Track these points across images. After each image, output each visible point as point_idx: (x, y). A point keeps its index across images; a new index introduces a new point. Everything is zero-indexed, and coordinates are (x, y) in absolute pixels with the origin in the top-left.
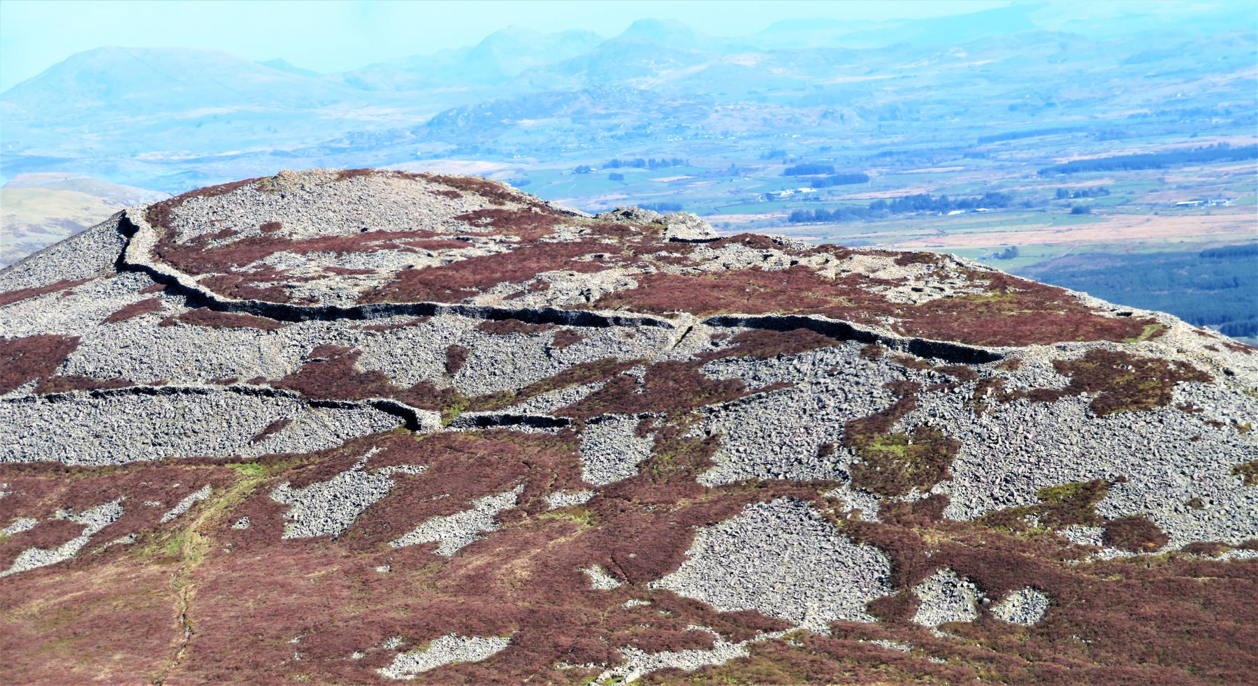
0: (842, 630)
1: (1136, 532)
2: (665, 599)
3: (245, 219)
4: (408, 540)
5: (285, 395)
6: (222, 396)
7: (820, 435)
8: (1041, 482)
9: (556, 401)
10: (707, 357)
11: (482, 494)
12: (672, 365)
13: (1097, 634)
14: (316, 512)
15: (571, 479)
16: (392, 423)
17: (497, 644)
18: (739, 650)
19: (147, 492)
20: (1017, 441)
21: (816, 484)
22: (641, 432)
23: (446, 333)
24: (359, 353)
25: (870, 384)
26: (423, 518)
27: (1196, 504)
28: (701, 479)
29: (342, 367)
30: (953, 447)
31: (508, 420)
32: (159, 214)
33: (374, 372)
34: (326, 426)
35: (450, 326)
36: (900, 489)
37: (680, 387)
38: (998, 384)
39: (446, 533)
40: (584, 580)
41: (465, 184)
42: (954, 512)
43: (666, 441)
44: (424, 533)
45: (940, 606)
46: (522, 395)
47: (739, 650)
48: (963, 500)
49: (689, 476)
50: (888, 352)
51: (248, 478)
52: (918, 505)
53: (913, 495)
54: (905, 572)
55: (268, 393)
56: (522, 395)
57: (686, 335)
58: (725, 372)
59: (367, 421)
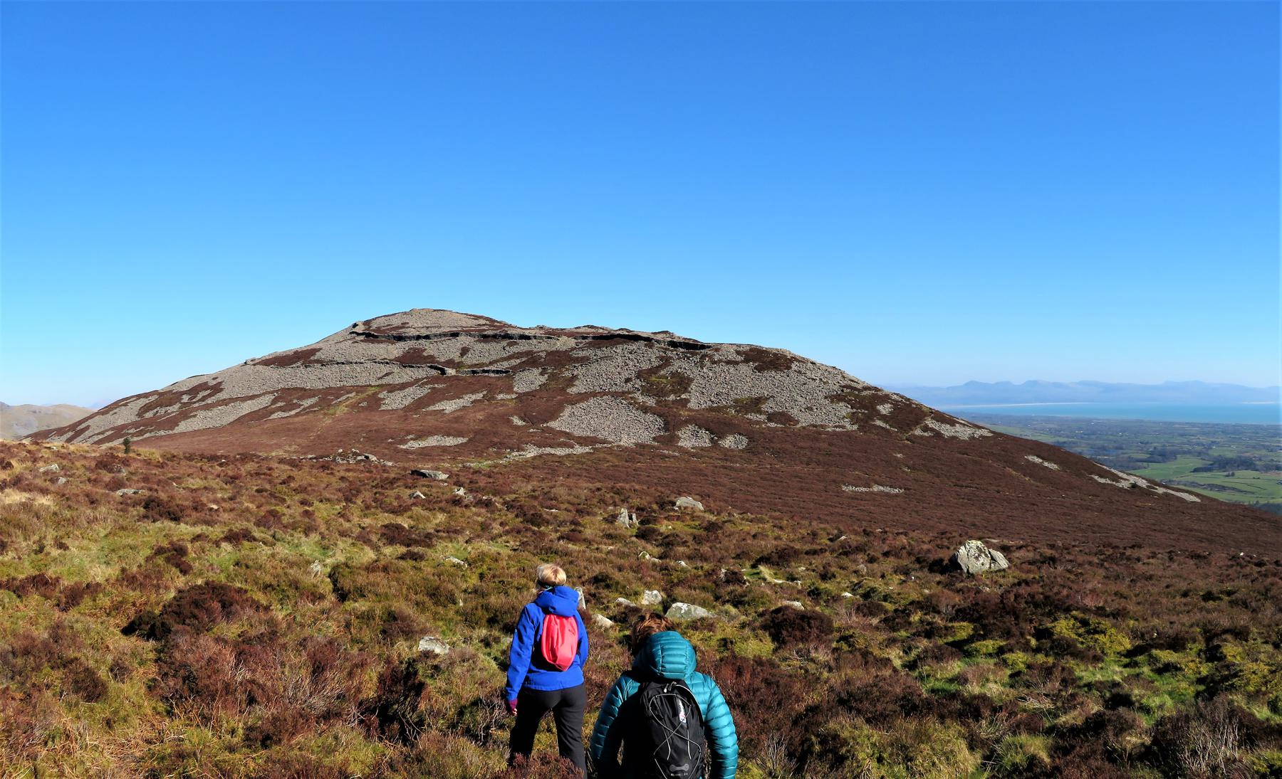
0: (641, 446)
1: (783, 418)
2: (551, 430)
3: (396, 322)
4: (431, 408)
6: (369, 365)
7: (625, 375)
8: (733, 395)
9: (505, 365)
10: (572, 349)
12: (557, 352)
13: (778, 453)
14: (395, 402)
15: (509, 390)
16: (434, 373)
17: (461, 440)
18: (587, 449)
19: (328, 396)
20: (722, 379)
21: (623, 393)
22: (542, 374)
25: (651, 357)
26: (439, 401)
27: (810, 409)
28: (569, 390)
30: (691, 380)
31: (484, 371)
32: (367, 323)
35: (464, 340)
36: (667, 394)
37: (560, 359)
38: (711, 357)
39: (449, 406)
40: (509, 422)
41: (481, 317)
42: (693, 405)
43: (553, 377)
44: (438, 407)
45: (688, 439)
46: (491, 363)
47: (587, 449)
48: (696, 400)
49: (563, 389)
50: (657, 345)
51: (370, 391)
52: (673, 402)
53: (672, 397)
54: (671, 425)
56: (491, 363)
57: (563, 344)
58: (581, 354)
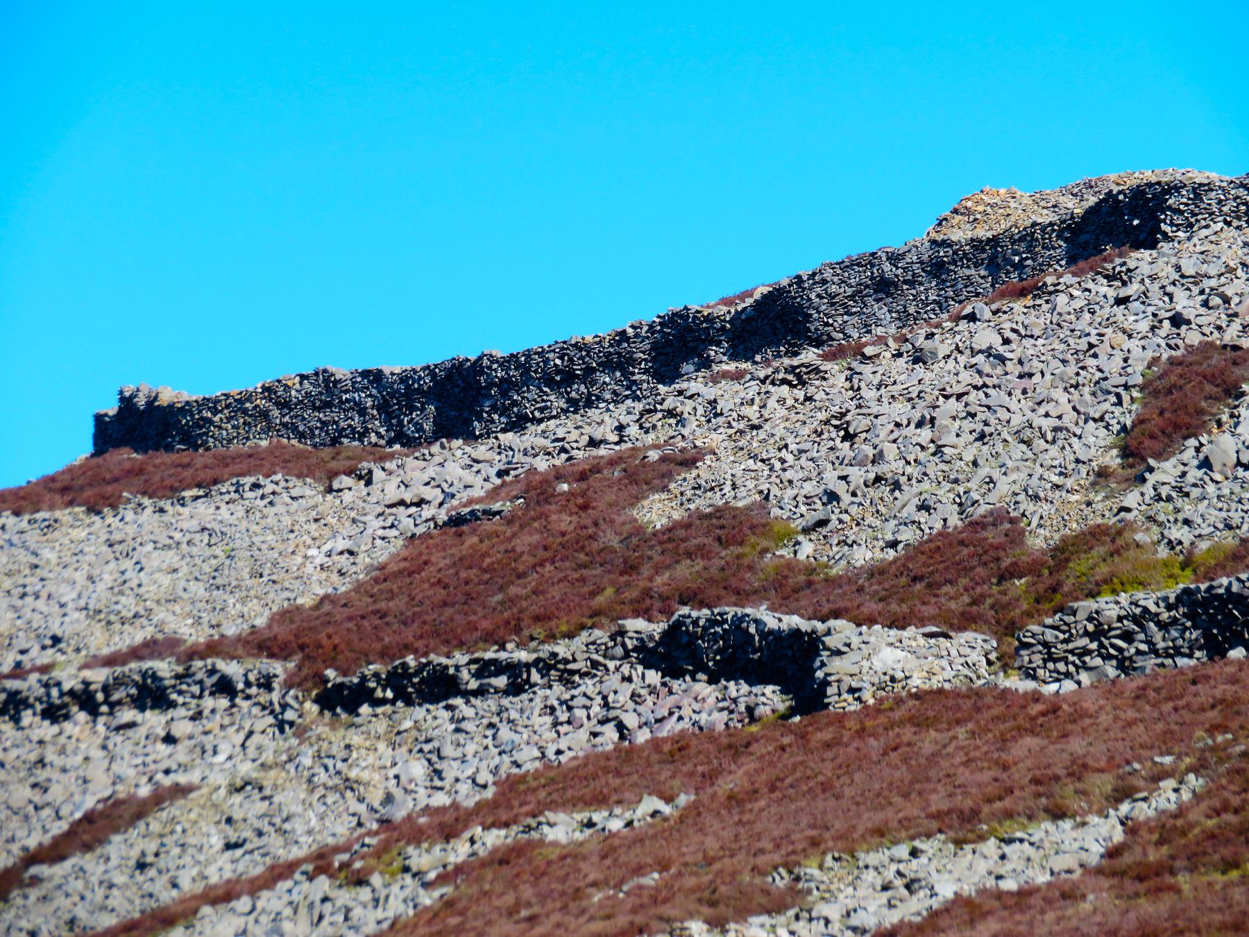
5: (225, 687)
11: (881, 835)
23: (1185, 303)
24: (689, 461)
29: (565, 522)
33: (718, 512)
34: (349, 785)
55: (152, 695)
59: (583, 735)
